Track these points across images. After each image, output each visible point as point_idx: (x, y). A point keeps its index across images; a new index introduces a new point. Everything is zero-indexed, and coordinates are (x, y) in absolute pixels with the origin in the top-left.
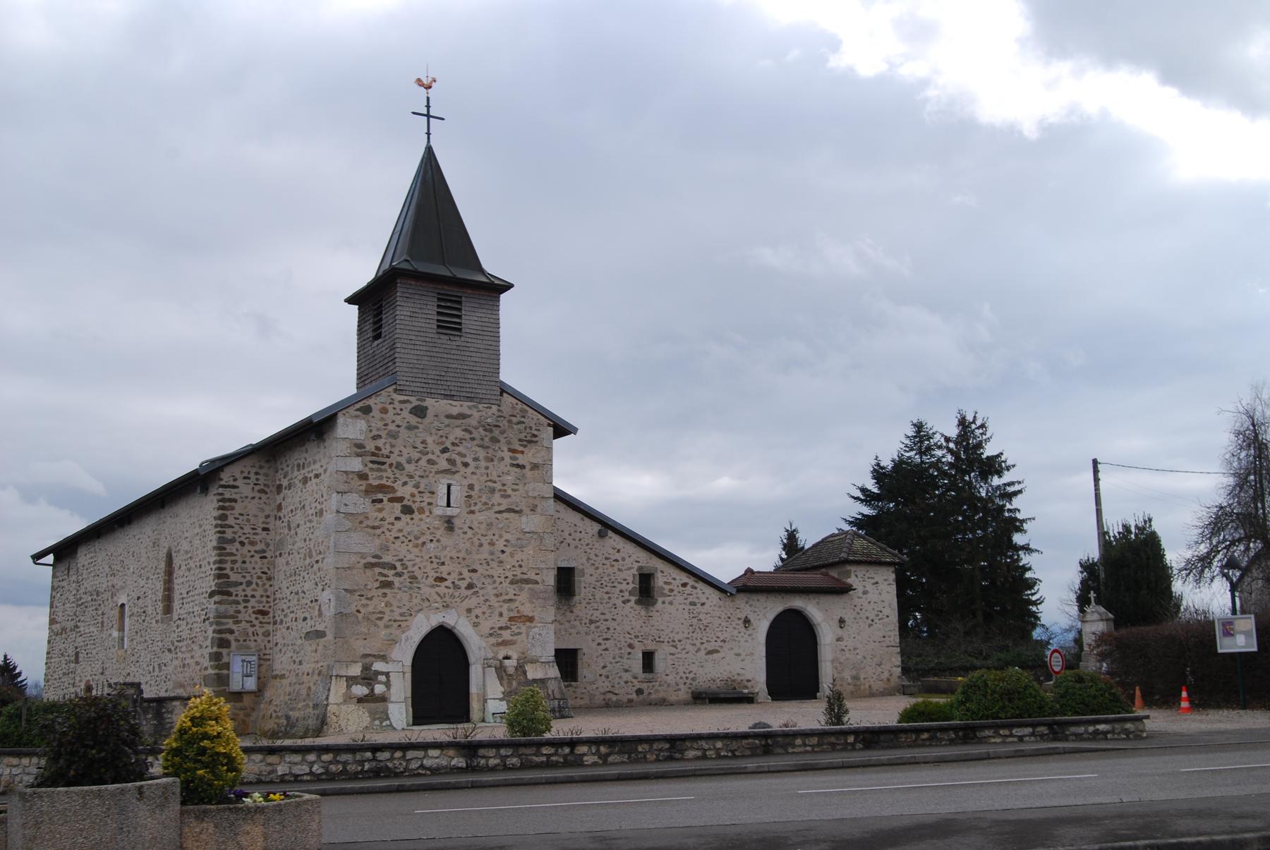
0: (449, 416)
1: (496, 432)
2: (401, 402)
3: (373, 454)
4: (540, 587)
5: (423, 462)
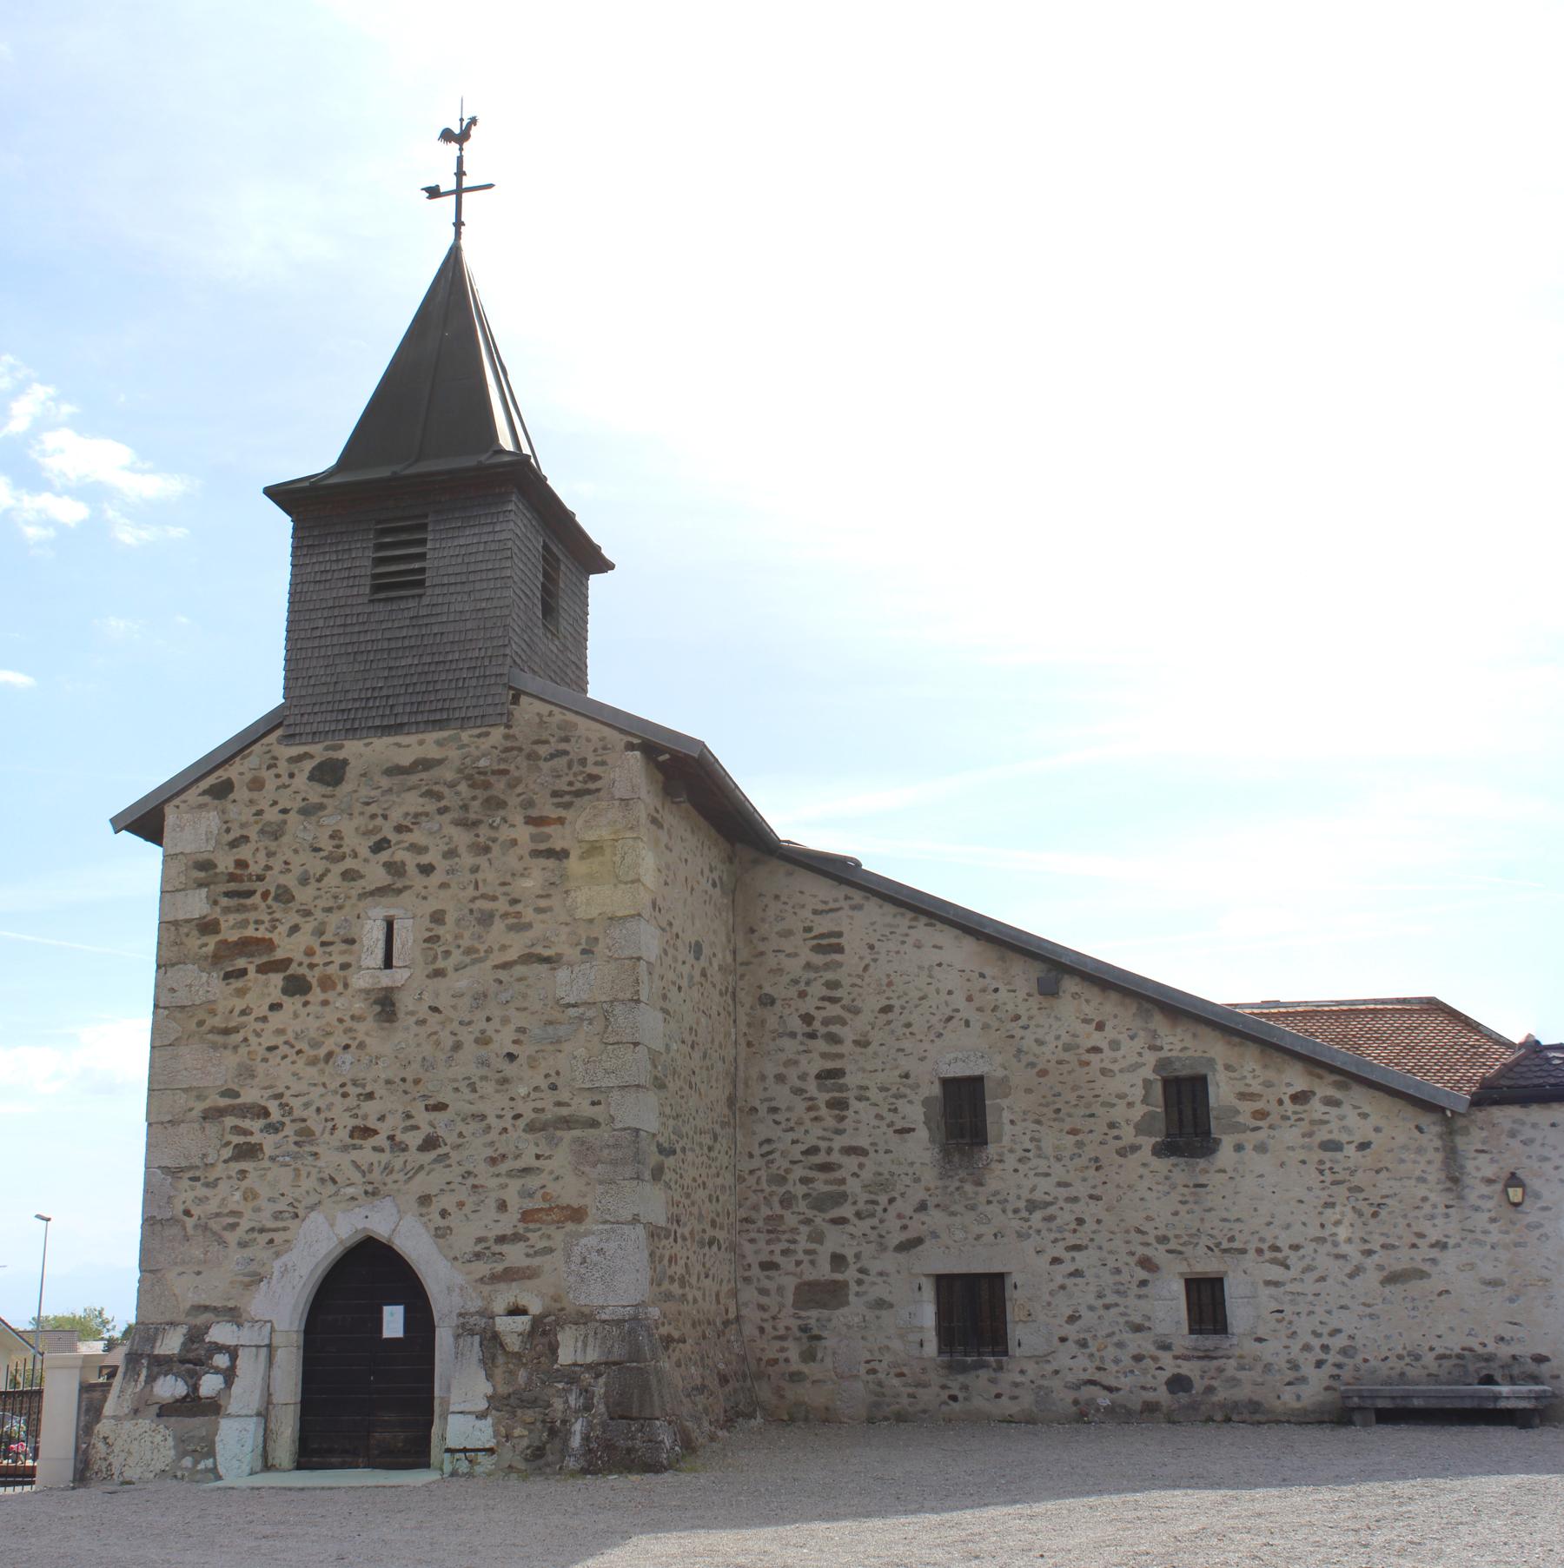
0: (395, 771)
1: (499, 785)
2: (292, 760)
3: (232, 878)
5: (333, 879)
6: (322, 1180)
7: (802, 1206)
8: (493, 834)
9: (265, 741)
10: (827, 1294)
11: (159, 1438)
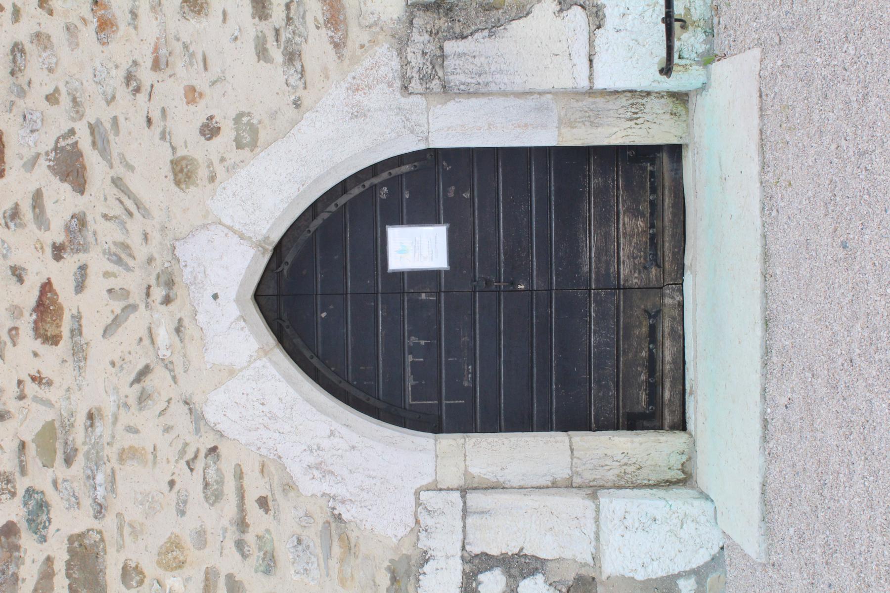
6: (143, 398)
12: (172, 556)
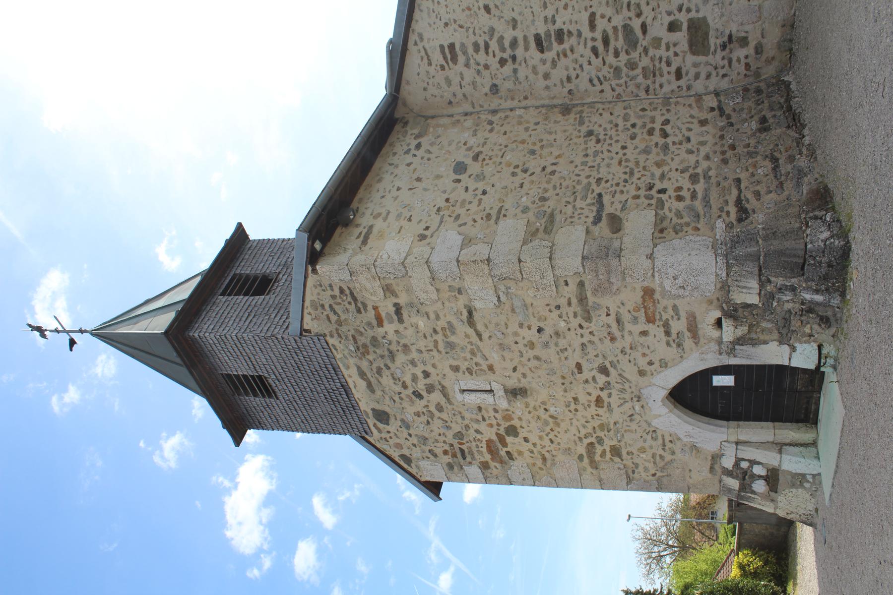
1: (362, 340)
3: (454, 456)
4: (588, 278)
5: (444, 416)
7: (635, 55)
8: (394, 343)
9: (373, 442)
10: (698, 35)
11: (790, 494)
12: (642, 450)
